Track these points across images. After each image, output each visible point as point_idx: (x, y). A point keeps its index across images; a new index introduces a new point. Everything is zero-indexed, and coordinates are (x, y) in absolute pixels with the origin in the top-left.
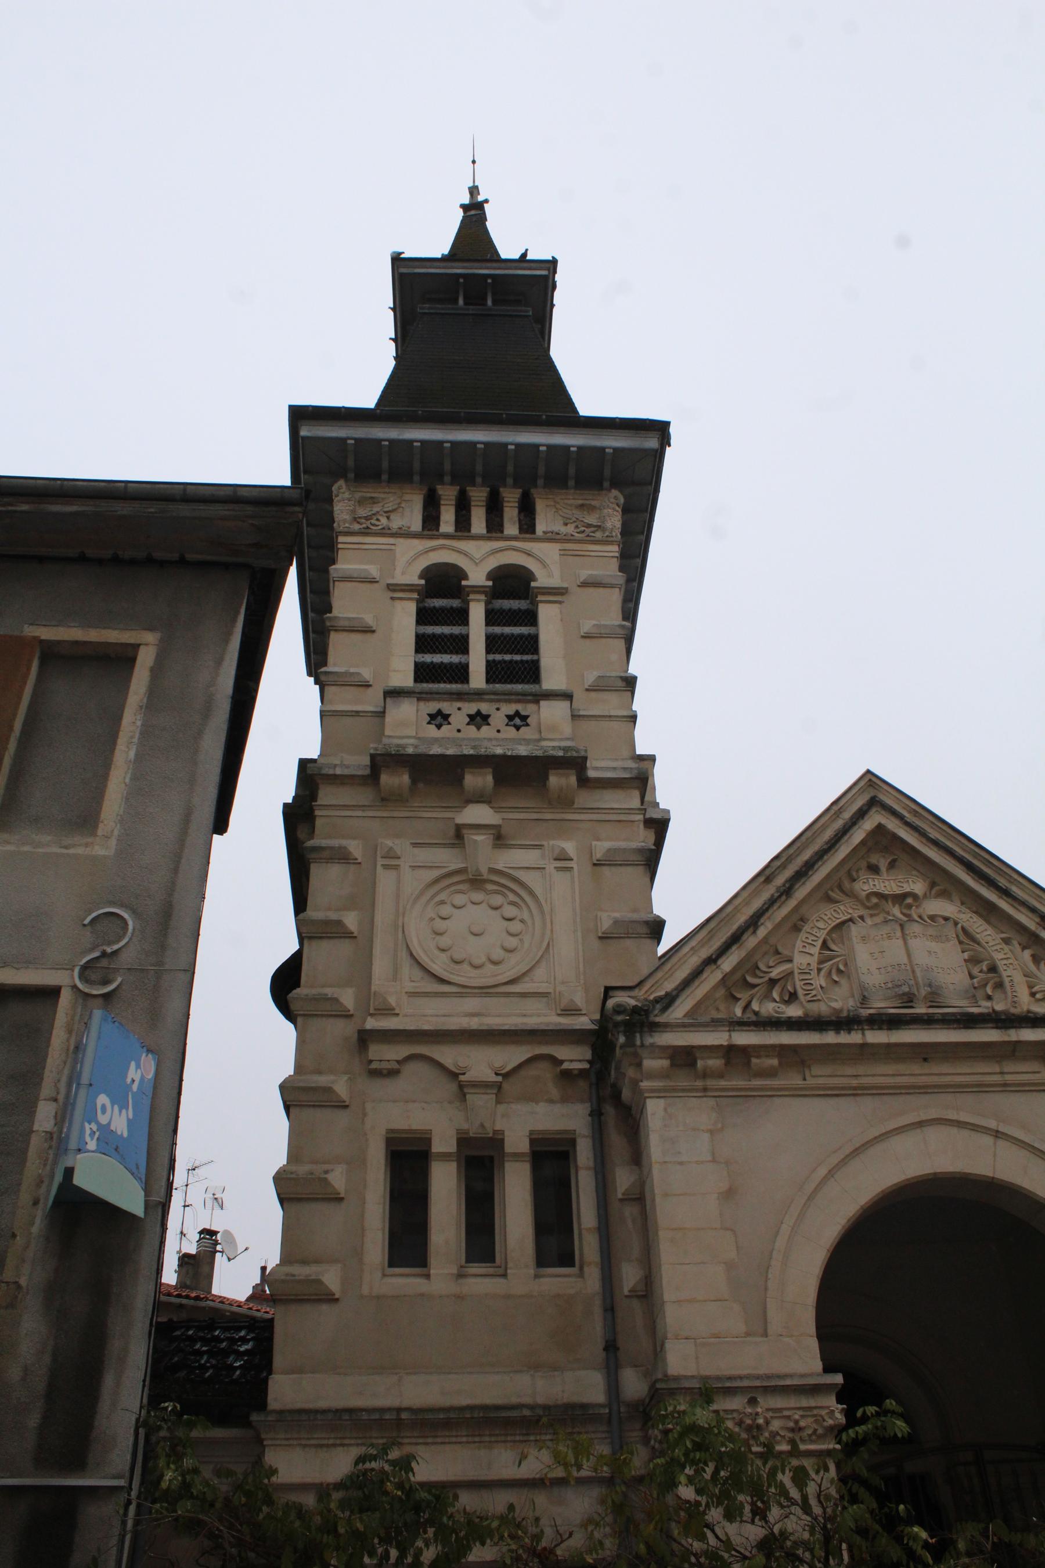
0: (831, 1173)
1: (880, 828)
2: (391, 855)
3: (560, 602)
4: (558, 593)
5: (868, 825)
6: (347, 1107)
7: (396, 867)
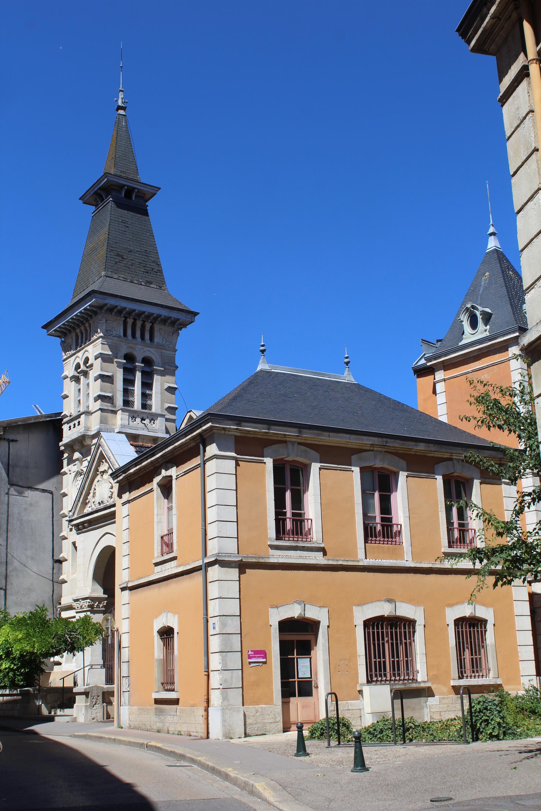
0: (94, 549)
1: (101, 451)
2: (70, 471)
3: (92, 369)
4: (92, 365)
5: (99, 451)
6: (67, 539)
7: (70, 474)
